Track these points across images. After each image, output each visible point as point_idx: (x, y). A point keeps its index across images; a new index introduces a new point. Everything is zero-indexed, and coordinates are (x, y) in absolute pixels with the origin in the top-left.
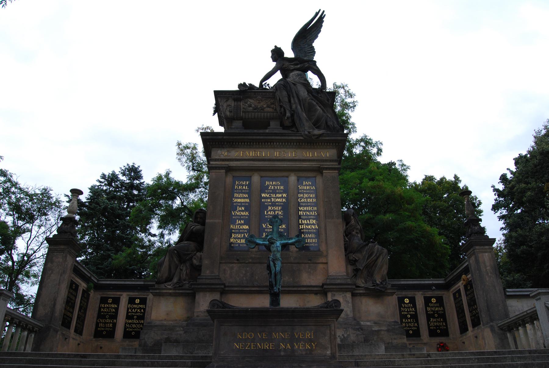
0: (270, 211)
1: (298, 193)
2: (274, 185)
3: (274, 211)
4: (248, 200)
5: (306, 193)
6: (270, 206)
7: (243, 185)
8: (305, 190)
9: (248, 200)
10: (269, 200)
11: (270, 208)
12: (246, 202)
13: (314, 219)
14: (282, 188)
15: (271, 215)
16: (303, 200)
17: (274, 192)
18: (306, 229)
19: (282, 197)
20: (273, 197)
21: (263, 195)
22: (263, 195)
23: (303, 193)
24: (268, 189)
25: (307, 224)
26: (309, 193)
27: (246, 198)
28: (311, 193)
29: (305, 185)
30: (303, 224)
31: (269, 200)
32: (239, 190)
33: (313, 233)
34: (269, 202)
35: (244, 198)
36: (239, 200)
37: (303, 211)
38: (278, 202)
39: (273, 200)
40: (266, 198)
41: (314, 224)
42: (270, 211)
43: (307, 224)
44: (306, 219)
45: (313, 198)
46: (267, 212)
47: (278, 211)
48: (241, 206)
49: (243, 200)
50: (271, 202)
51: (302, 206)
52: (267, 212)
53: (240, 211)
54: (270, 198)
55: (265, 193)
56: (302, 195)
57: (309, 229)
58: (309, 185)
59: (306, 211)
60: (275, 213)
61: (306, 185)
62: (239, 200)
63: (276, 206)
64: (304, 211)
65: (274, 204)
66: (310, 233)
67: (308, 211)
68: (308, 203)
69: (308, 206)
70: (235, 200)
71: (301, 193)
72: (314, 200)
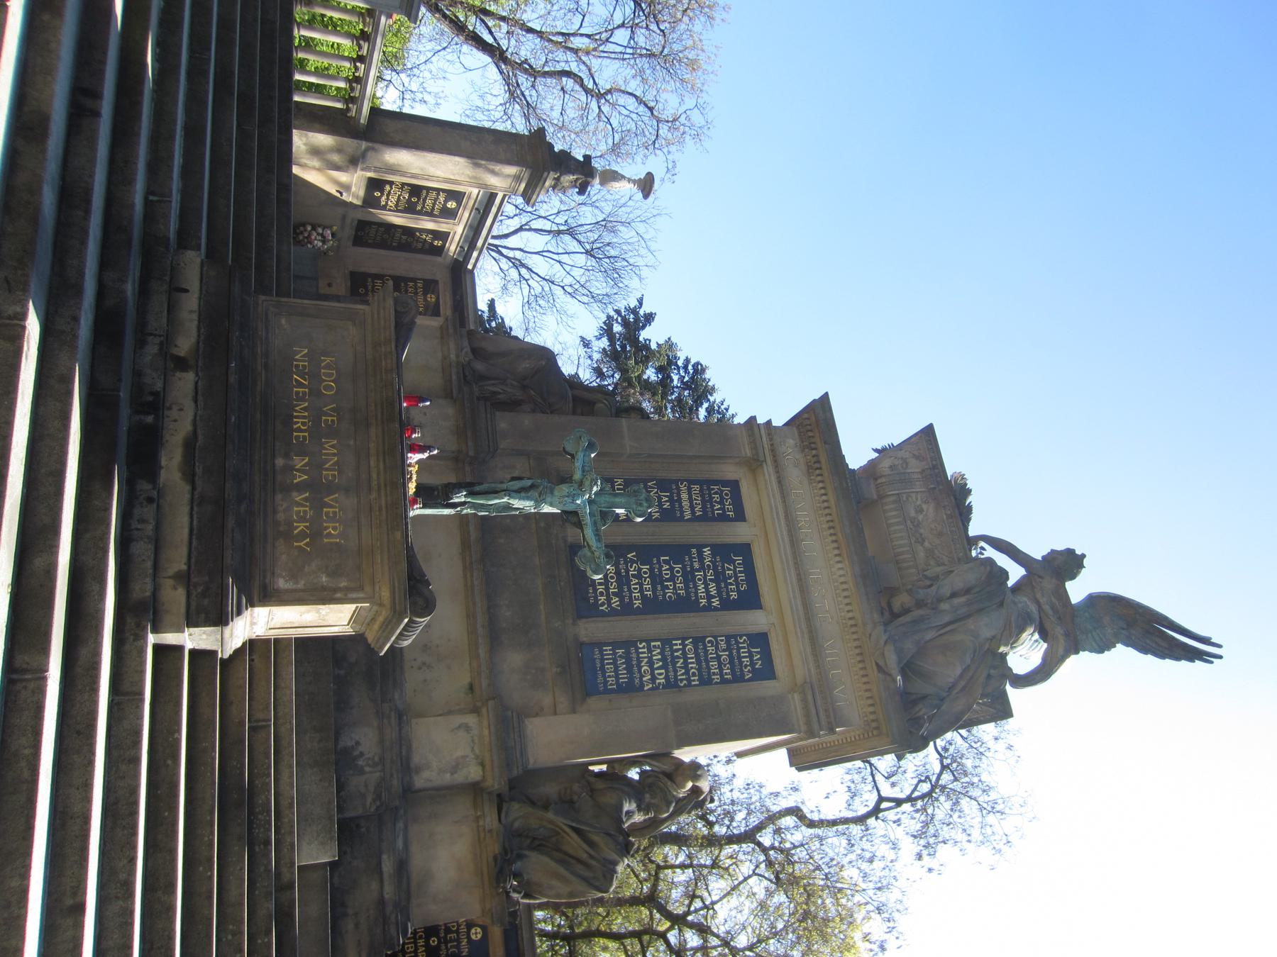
0: (671, 569)
1: (728, 638)
2: (737, 578)
3: (672, 579)
4: (688, 515)
5: (730, 656)
6: (684, 568)
7: (721, 502)
8: (738, 652)
9: (688, 515)
10: (696, 565)
11: (678, 567)
12: (682, 512)
13: (667, 678)
14: (734, 595)
15: (660, 571)
16: (711, 649)
17: (720, 578)
18: (638, 658)
19: (709, 597)
20: (705, 576)
21: (707, 551)
22: (707, 551)
23: (729, 649)
24: (723, 562)
25: (651, 663)
26: (732, 662)
27: (693, 512)
28: (732, 669)
29: (749, 652)
30: (650, 651)
31: (696, 565)
32: (710, 495)
33: (631, 679)
34: (692, 566)
35: (692, 507)
36: (685, 496)
37: (683, 650)
38: (696, 587)
39: (699, 574)
40: (701, 559)
41: (653, 679)
42: (671, 569)
43: (651, 663)
44: (664, 659)
45: (721, 674)
46: (666, 562)
47: (675, 588)
48: (671, 500)
49: (686, 504)
50: (693, 570)
51: (696, 648)
52: (666, 562)
53: (660, 498)
54: (702, 568)
55: (713, 555)
56: (723, 645)
57: (640, 668)
58: (753, 664)
59: (686, 658)
60: (667, 580)
61: (751, 656)
62: (685, 496)
63: (686, 582)
64: (684, 654)
65: (689, 577)
66: (629, 669)
67: (686, 664)
68: (707, 661)
69: (699, 662)
70: (683, 488)
71: (728, 642)
72: (716, 678)
